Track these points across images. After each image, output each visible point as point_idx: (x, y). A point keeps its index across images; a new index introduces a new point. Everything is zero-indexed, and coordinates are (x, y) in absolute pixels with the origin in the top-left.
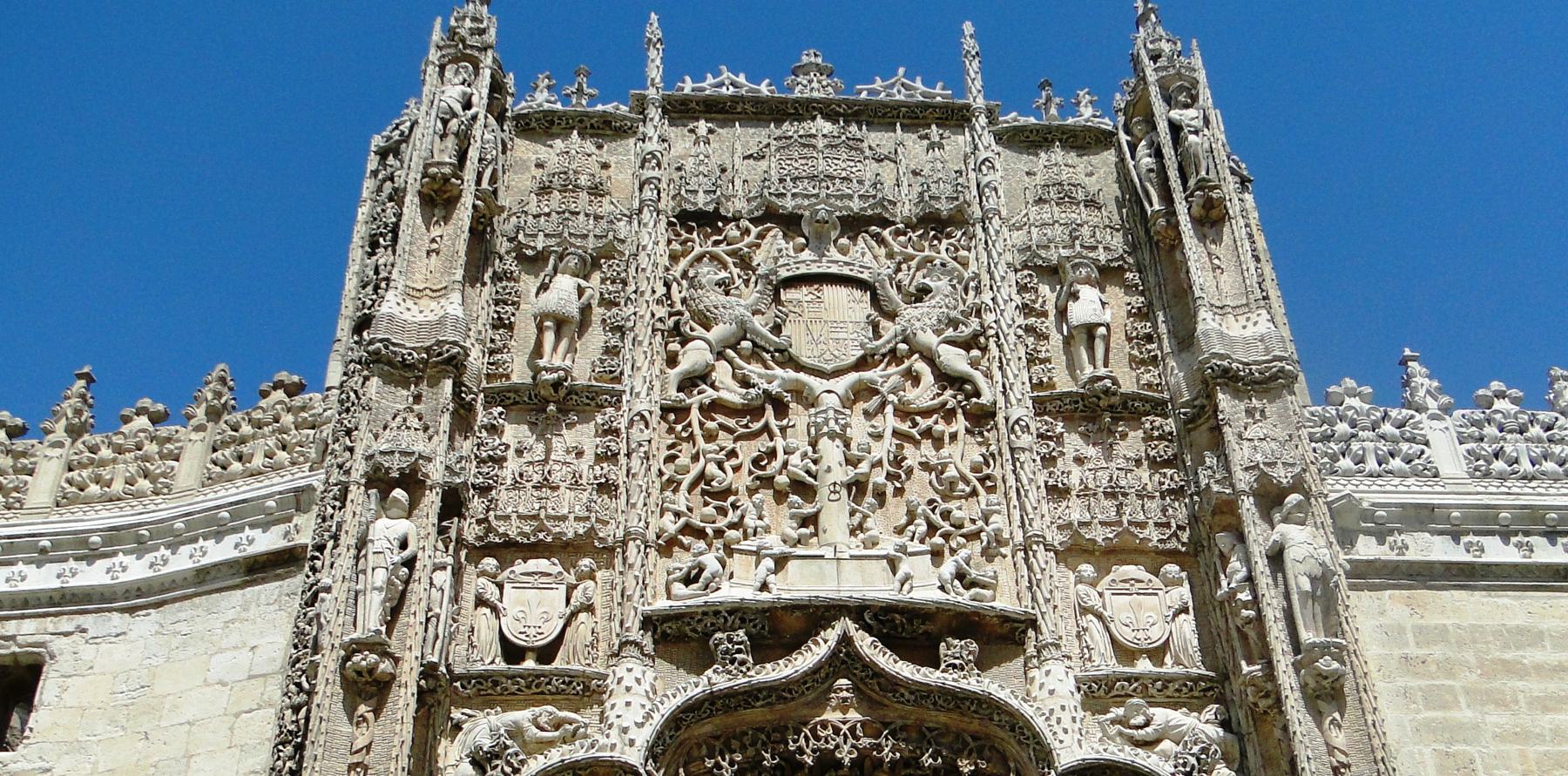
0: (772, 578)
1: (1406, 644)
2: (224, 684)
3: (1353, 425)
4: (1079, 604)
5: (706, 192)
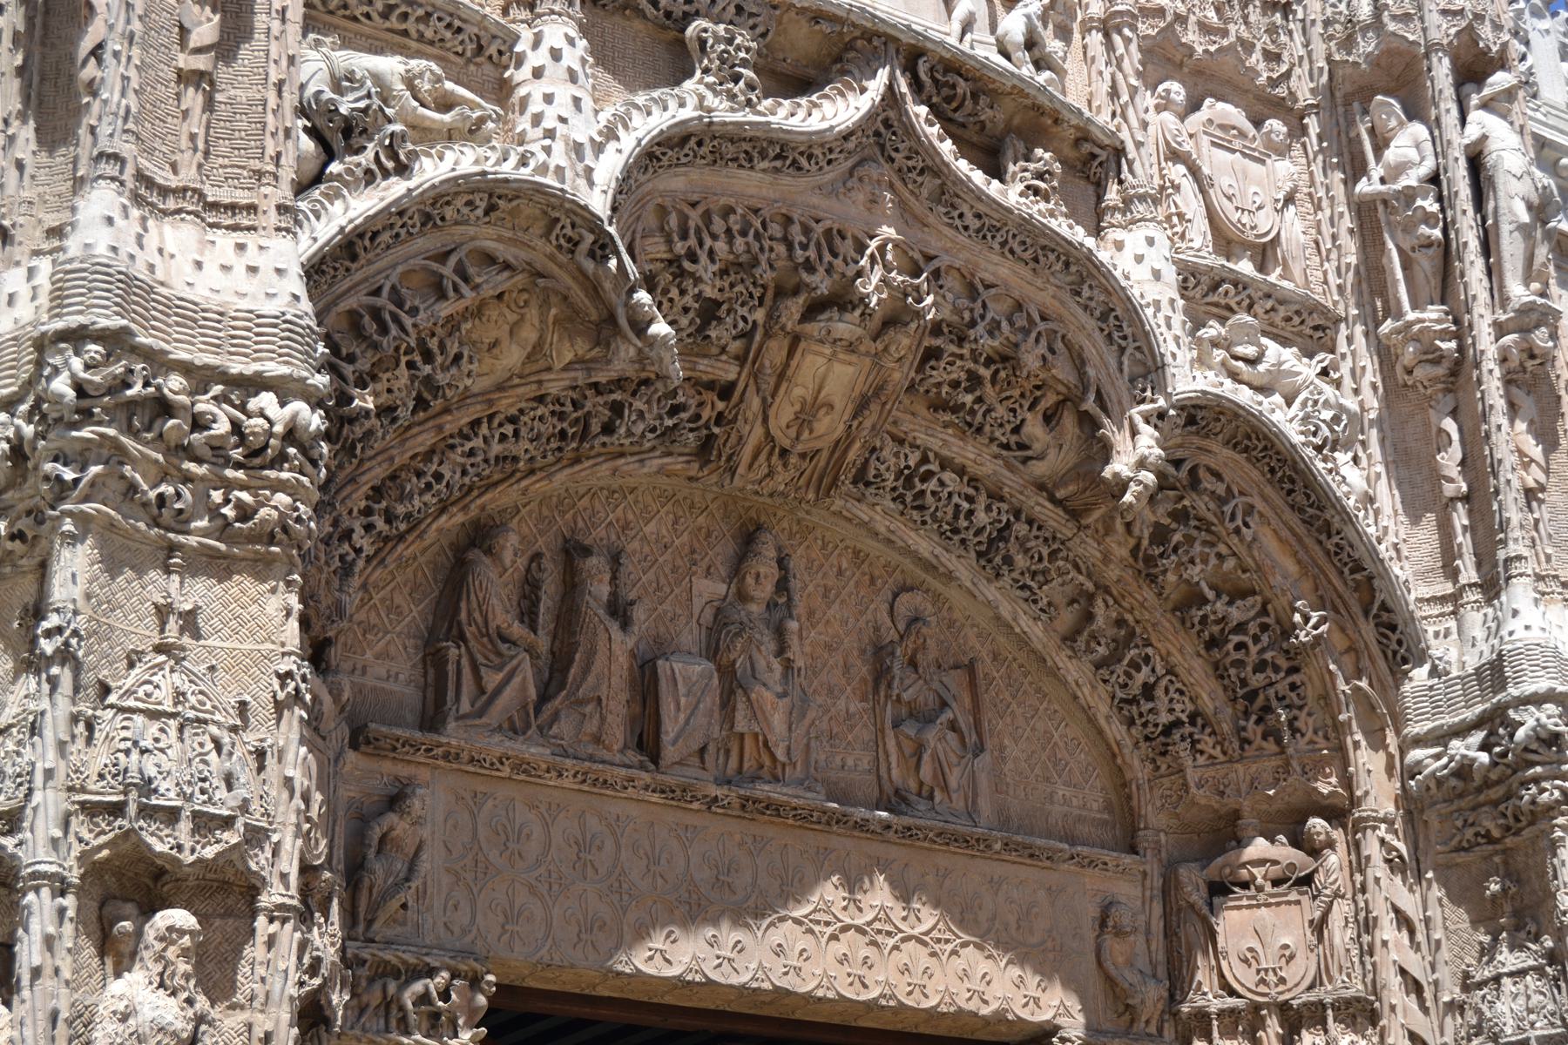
4: (1167, 143)
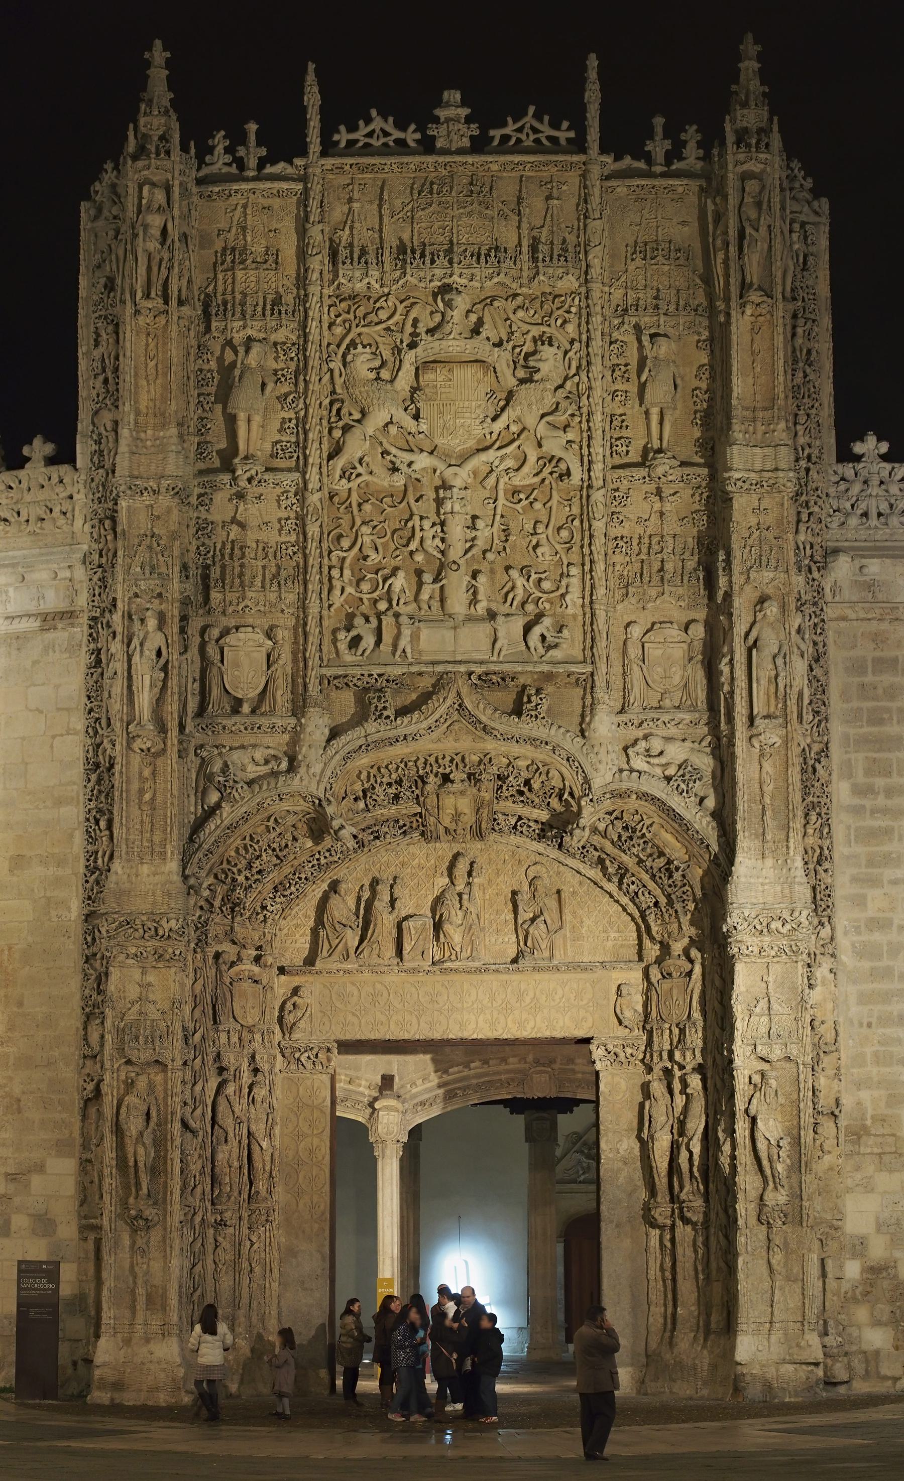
2: (41, 712)
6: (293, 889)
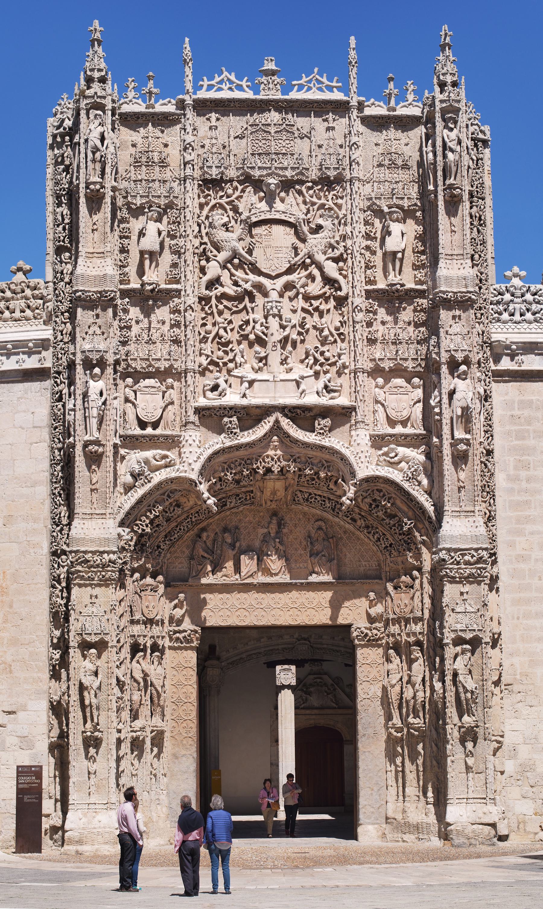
0: (247, 392)
1: (514, 409)
2: (23, 429)
3: (513, 295)
5: (217, 167)
6: (176, 536)
